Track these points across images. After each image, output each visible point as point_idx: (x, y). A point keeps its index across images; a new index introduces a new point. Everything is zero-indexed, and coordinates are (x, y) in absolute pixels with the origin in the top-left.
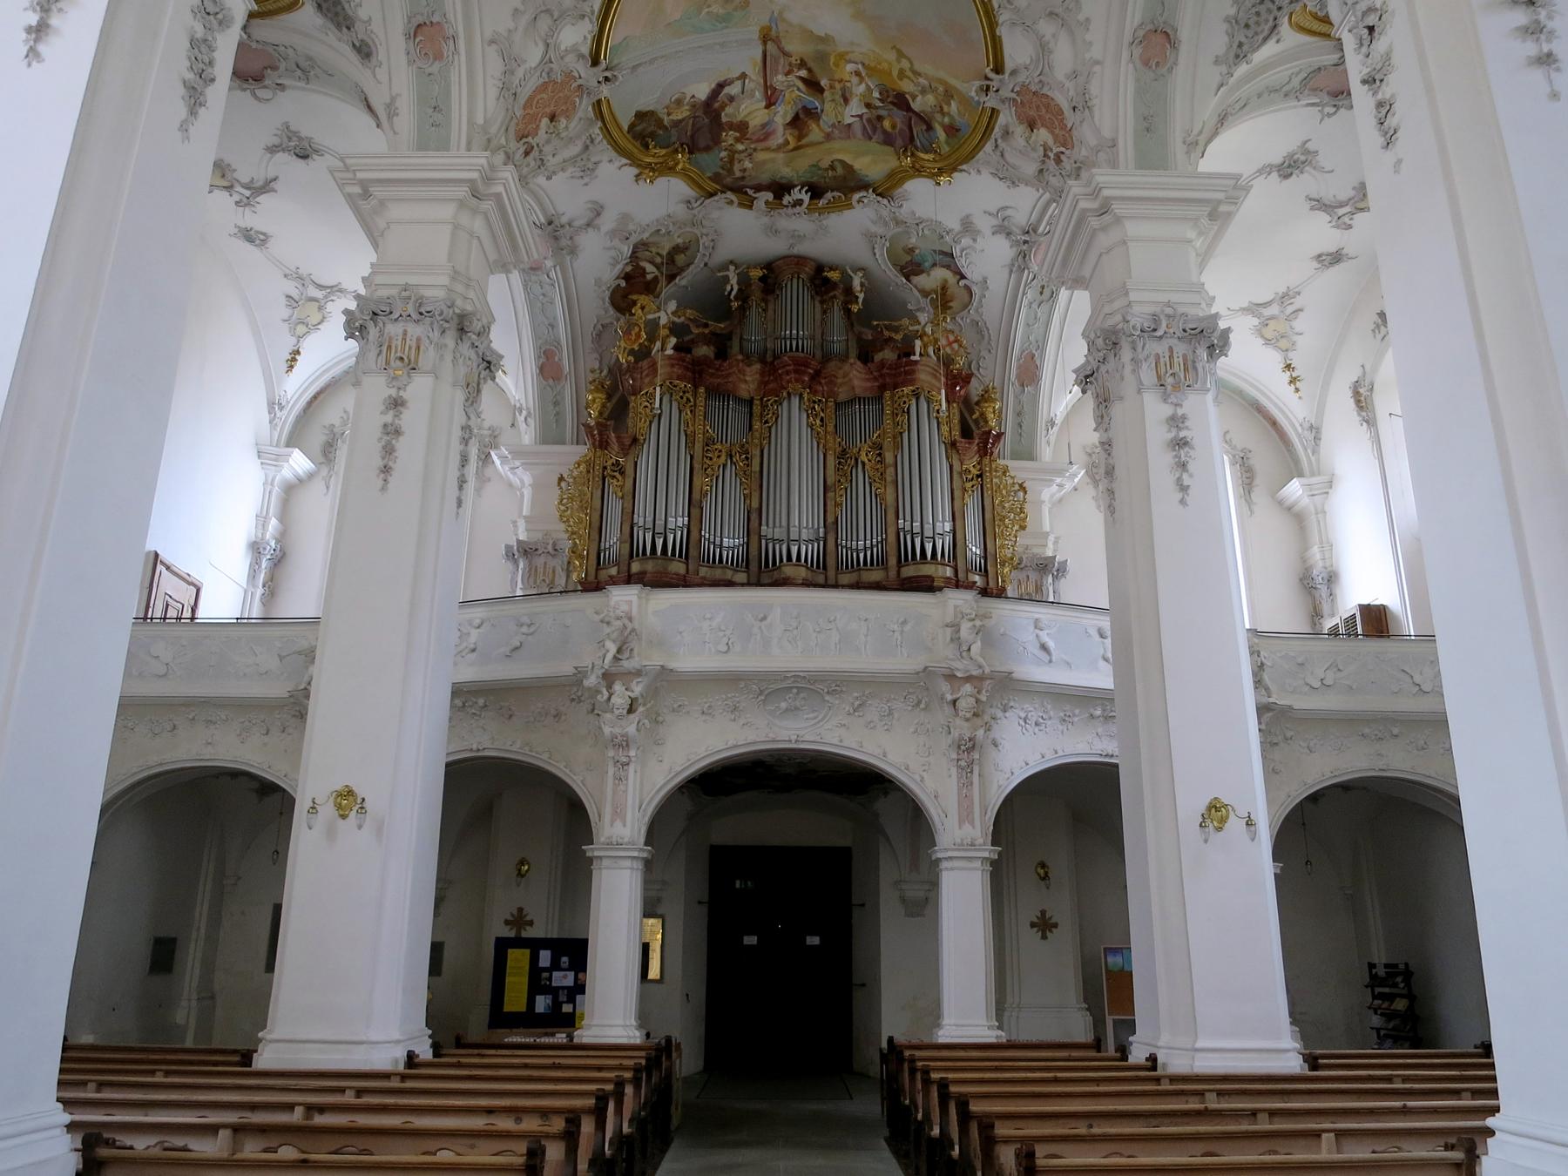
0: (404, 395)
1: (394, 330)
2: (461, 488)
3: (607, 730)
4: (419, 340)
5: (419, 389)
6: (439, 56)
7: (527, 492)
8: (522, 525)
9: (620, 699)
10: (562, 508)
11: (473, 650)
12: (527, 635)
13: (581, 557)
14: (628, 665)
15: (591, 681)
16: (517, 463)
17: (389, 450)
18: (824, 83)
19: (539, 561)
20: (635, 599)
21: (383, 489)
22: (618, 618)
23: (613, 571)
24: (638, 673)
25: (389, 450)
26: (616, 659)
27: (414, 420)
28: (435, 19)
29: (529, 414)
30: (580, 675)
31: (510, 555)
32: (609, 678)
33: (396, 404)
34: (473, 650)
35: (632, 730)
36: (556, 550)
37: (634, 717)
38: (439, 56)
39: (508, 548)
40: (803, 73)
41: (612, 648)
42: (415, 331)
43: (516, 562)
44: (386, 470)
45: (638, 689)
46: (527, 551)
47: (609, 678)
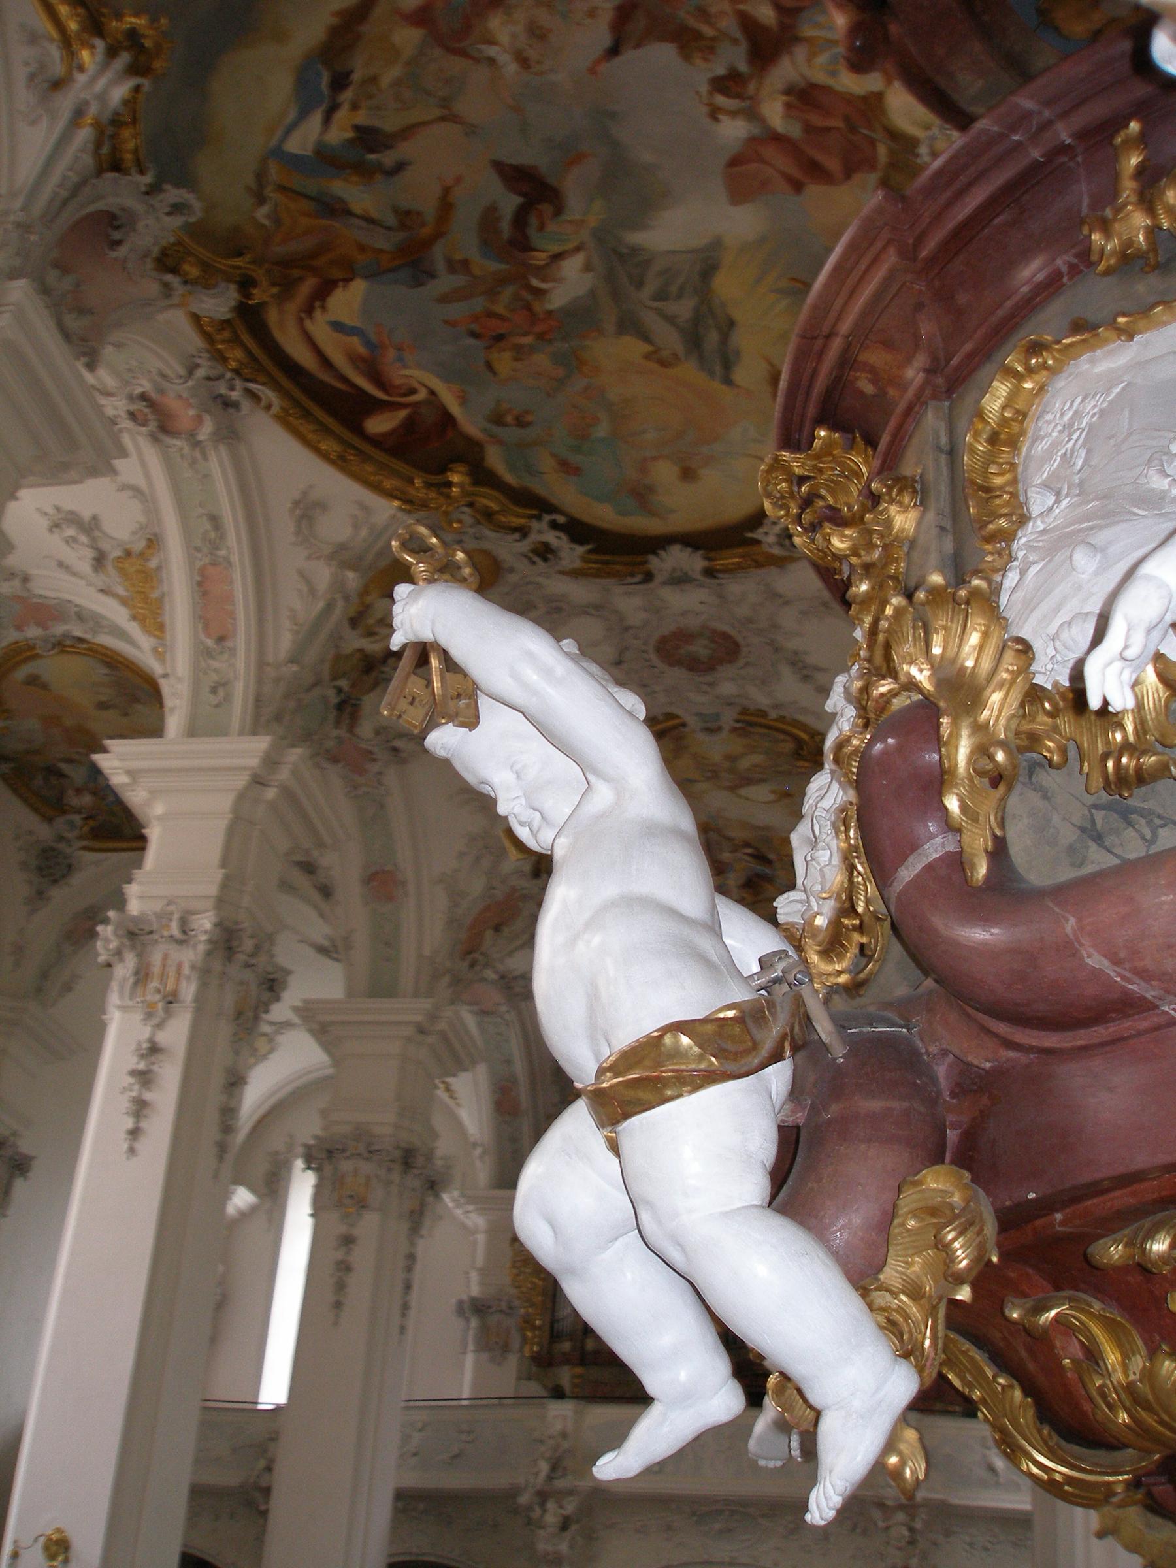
0: (356, 1232)
1: (346, 1166)
2: (404, 1315)
3: (541, 1547)
4: (368, 1178)
5: (369, 1225)
6: (390, 898)
7: (481, 1238)
8: (474, 1276)
9: (551, 1518)
10: (515, 1271)
11: (415, 1454)
12: (469, 1442)
13: (534, 1328)
14: (560, 1484)
15: (524, 1499)
16: (471, 1208)
17: (340, 1286)
18: (772, 856)
19: (493, 1319)
20: (570, 1413)
21: (336, 1323)
22: (551, 1437)
23: (566, 1346)
24: (571, 1492)
25: (340, 1286)
26: (550, 1478)
27: (363, 1257)
28: (389, 867)
29: (484, 1153)
30: (512, 1493)
31: (460, 1309)
32: (543, 1496)
33: (348, 1241)
34: (415, 1454)
35: (564, 1547)
36: (510, 1308)
37: (568, 1535)
38: (390, 898)
39: (460, 1303)
40: (749, 851)
41: (544, 1467)
42: (366, 1168)
43: (468, 1320)
44: (338, 1305)
45: (570, 1507)
46: (479, 1308)
47: (543, 1496)
